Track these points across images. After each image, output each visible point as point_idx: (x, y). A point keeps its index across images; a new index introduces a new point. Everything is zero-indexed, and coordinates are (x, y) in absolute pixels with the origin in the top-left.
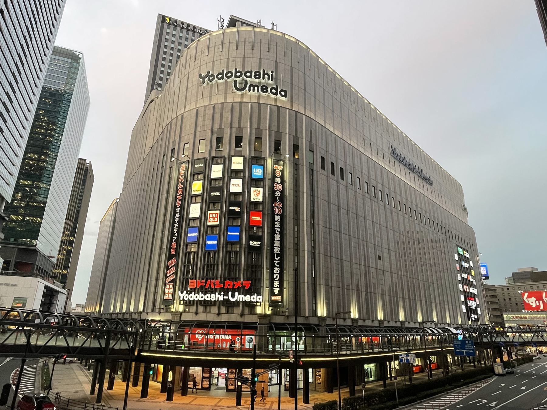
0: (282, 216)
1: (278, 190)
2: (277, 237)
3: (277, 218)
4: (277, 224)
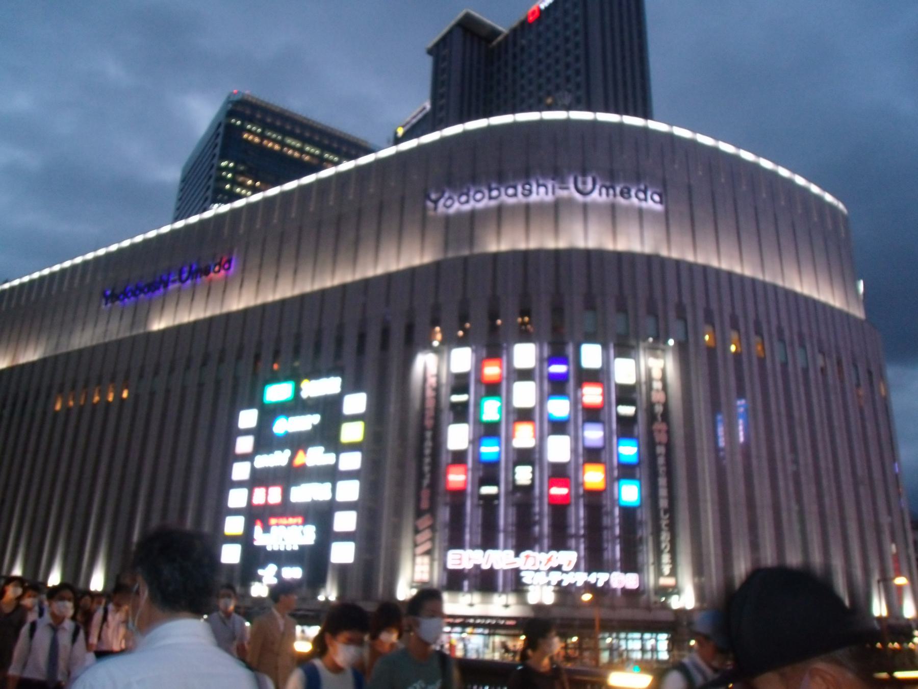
0: (669, 446)
1: (658, 402)
2: (662, 481)
3: (661, 450)
4: (661, 461)
